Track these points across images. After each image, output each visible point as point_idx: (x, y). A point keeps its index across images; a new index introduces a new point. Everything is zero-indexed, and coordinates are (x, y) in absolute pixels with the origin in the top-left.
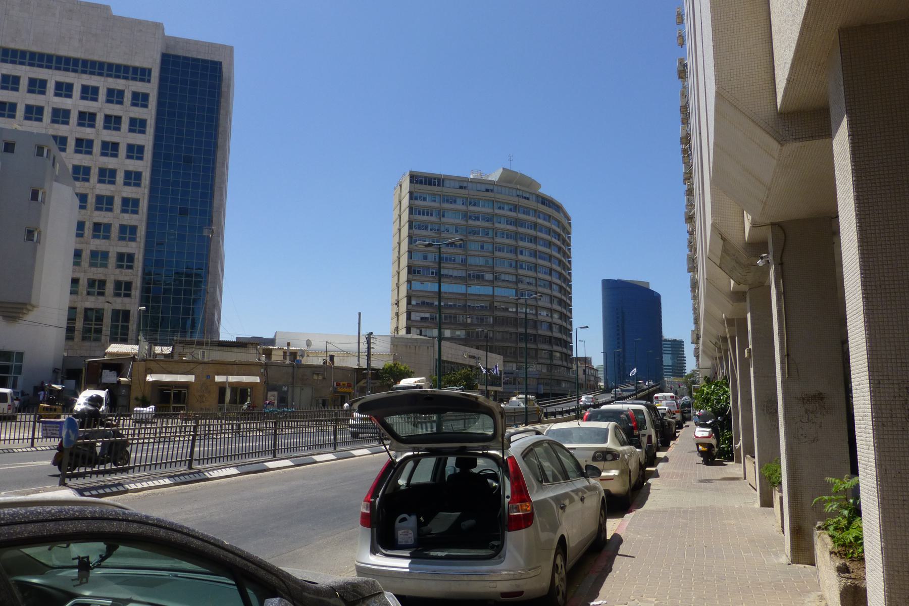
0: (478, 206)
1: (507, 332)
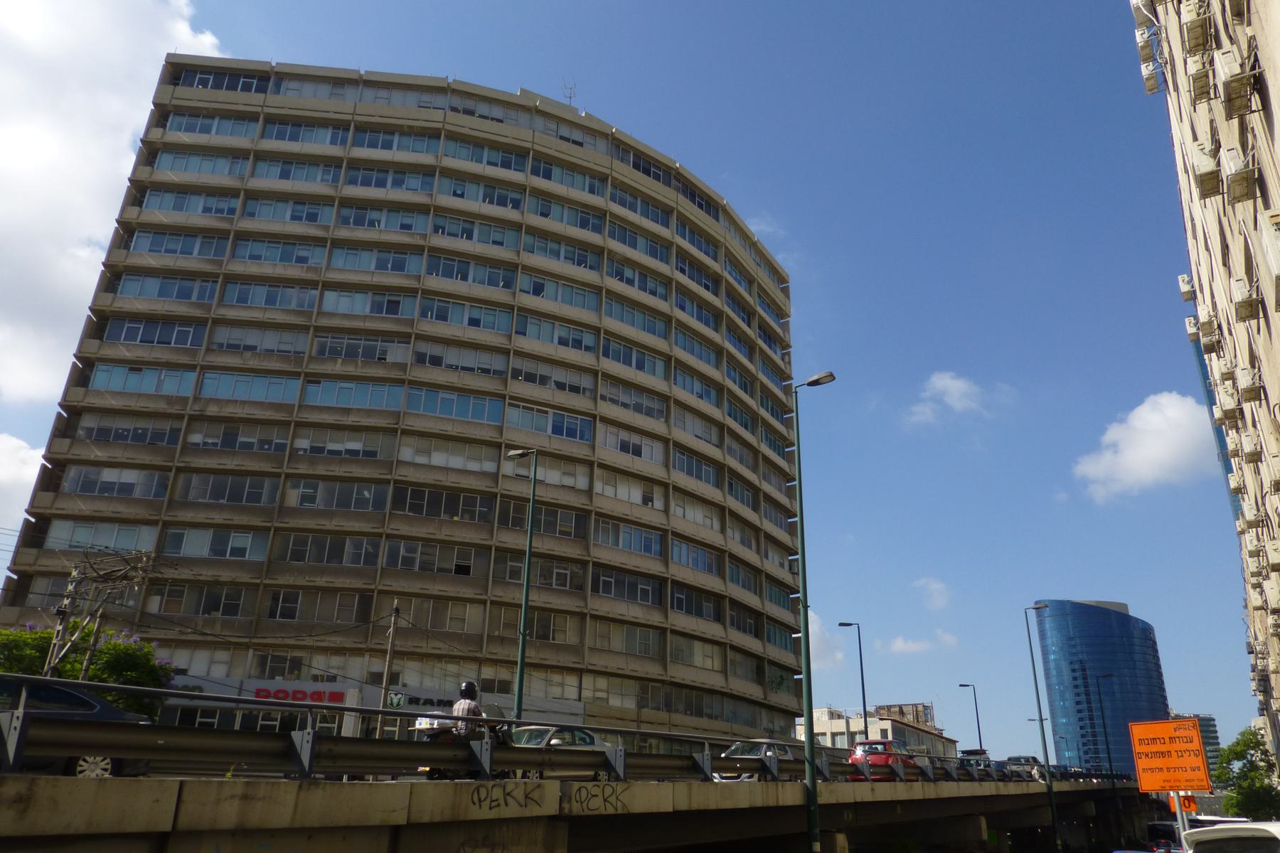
0: (387, 146)
1: (447, 545)
